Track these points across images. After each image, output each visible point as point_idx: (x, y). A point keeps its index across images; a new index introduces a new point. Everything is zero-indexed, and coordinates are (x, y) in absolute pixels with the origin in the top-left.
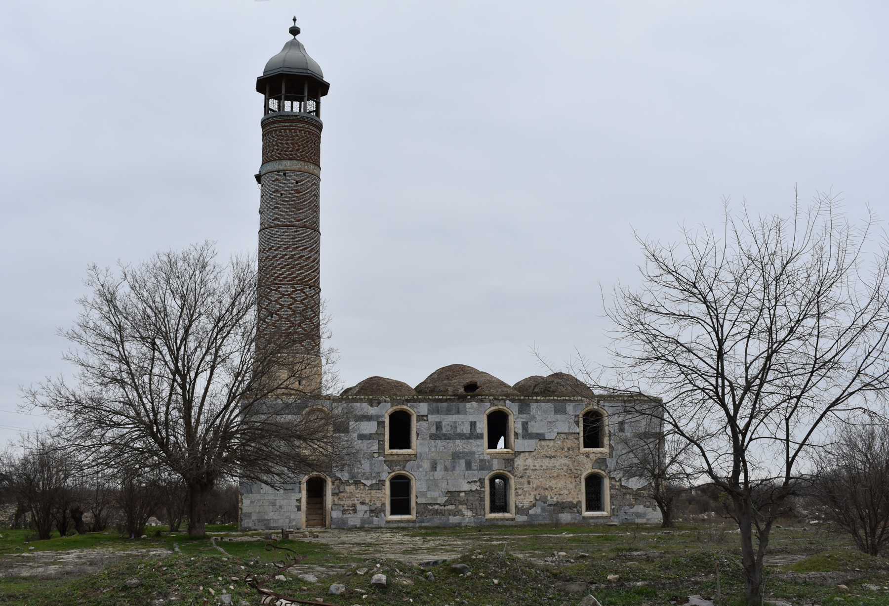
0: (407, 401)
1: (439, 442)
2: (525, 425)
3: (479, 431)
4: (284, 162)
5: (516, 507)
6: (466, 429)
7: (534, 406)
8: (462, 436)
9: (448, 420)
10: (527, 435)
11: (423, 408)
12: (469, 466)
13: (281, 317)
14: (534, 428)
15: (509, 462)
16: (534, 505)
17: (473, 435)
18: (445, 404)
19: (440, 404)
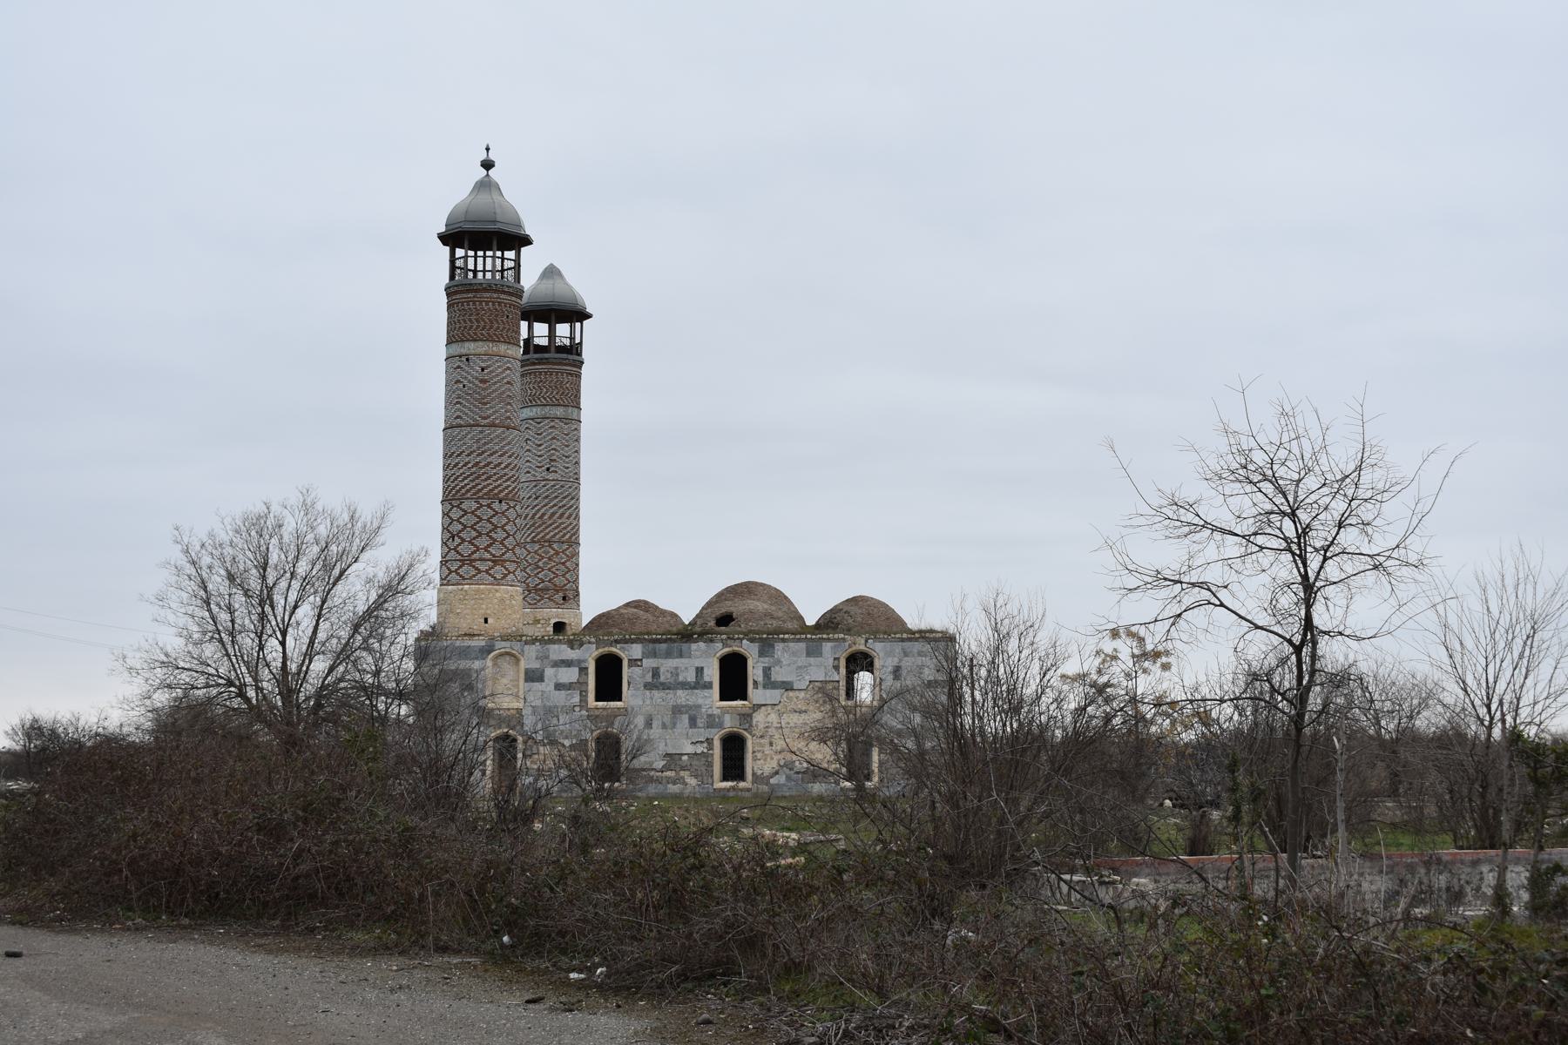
0: (617, 642)
1: (655, 693)
2: (767, 672)
3: (706, 679)
4: (467, 344)
5: (754, 774)
6: (691, 677)
7: (779, 646)
8: (684, 685)
9: (667, 665)
10: (769, 684)
11: (636, 650)
12: (693, 722)
13: (463, 540)
14: (778, 675)
15: (746, 717)
16: (777, 773)
17: (700, 684)
18: (664, 646)
19: (657, 646)
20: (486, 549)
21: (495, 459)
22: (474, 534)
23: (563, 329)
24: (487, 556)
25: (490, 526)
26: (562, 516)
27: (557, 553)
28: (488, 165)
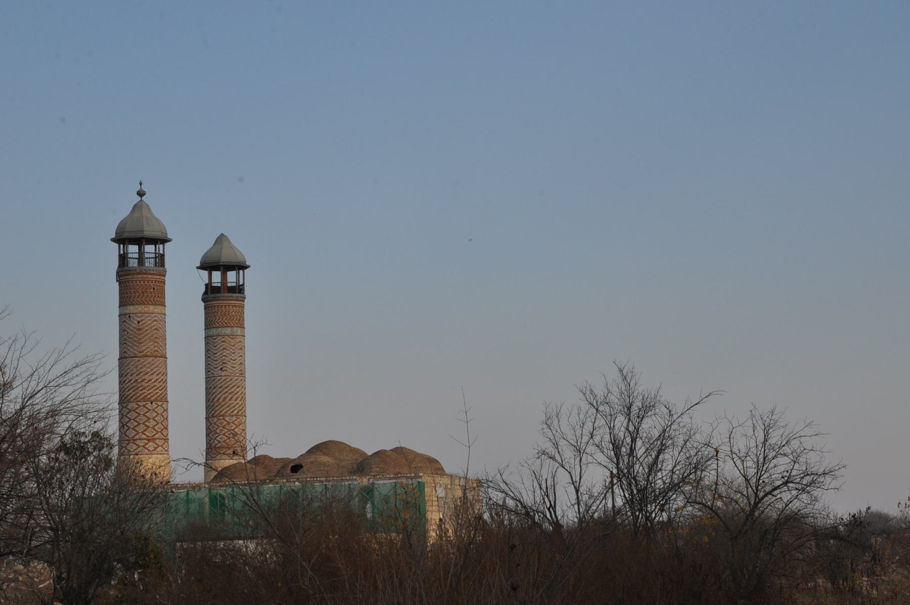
13: (129, 428)
20: (143, 433)
21: (147, 377)
22: (136, 424)
23: (231, 276)
24: (144, 437)
25: (145, 419)
26: (230, 400)
27: (229, 423)
28: (141, 194)
